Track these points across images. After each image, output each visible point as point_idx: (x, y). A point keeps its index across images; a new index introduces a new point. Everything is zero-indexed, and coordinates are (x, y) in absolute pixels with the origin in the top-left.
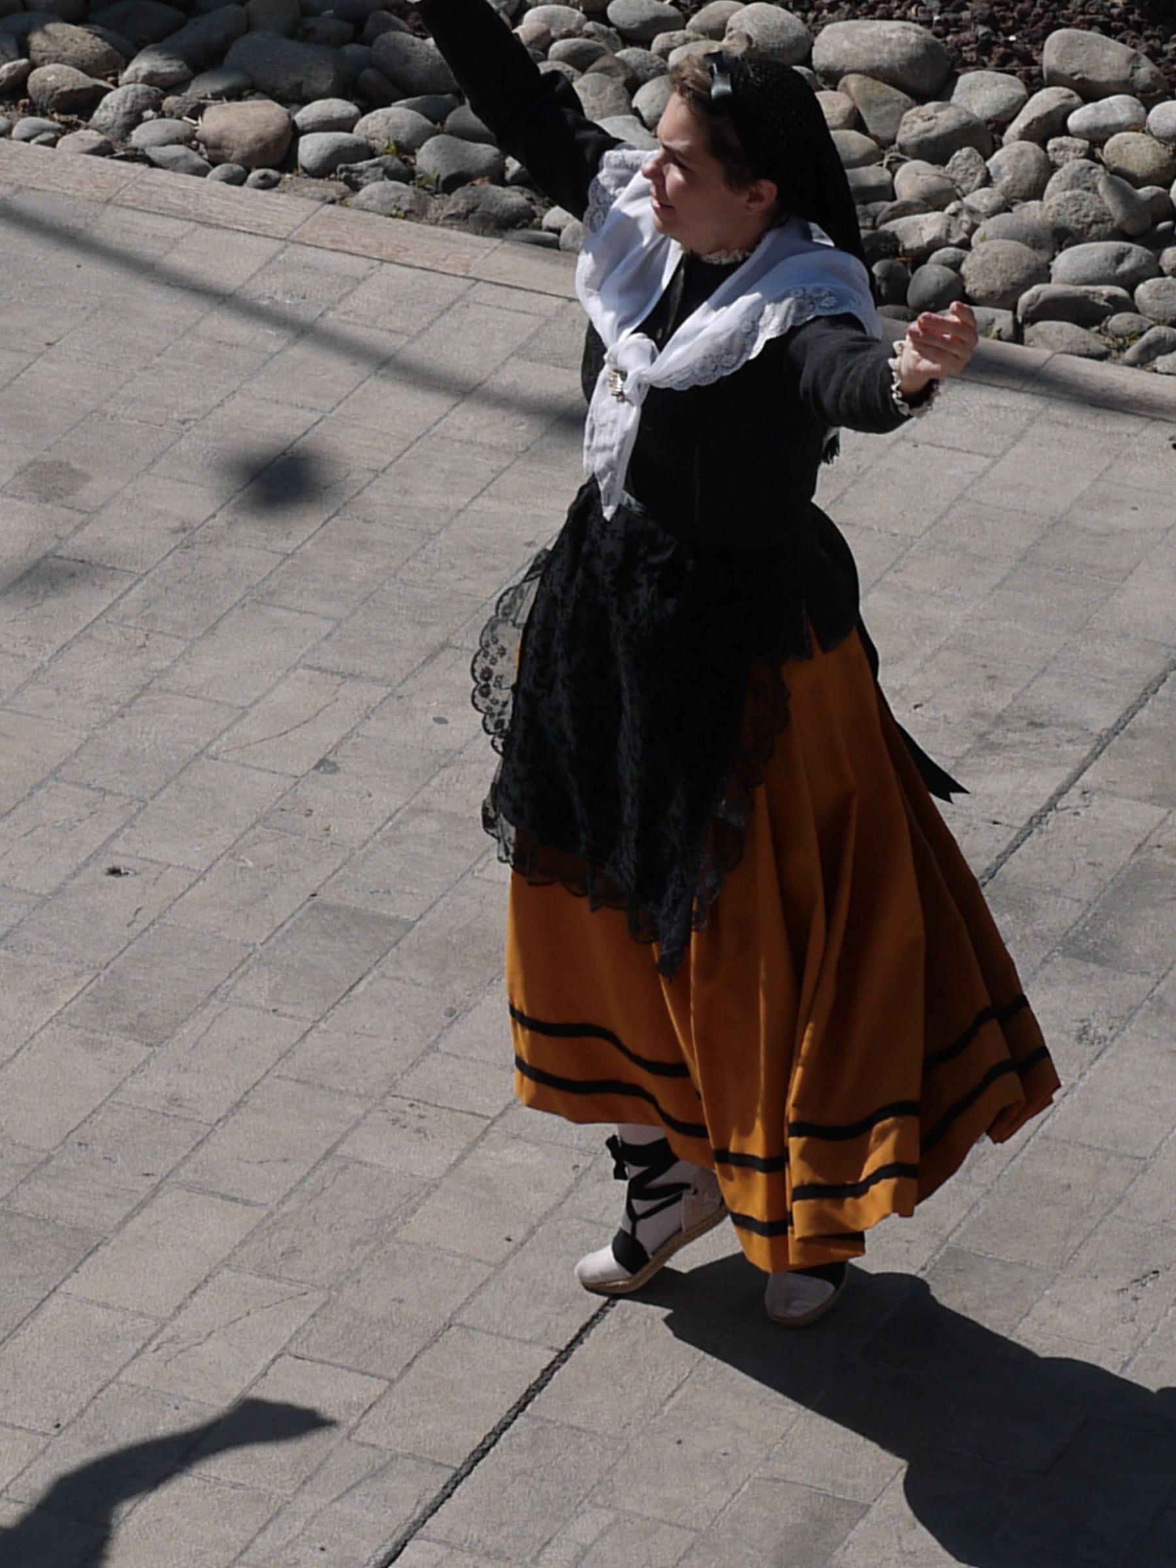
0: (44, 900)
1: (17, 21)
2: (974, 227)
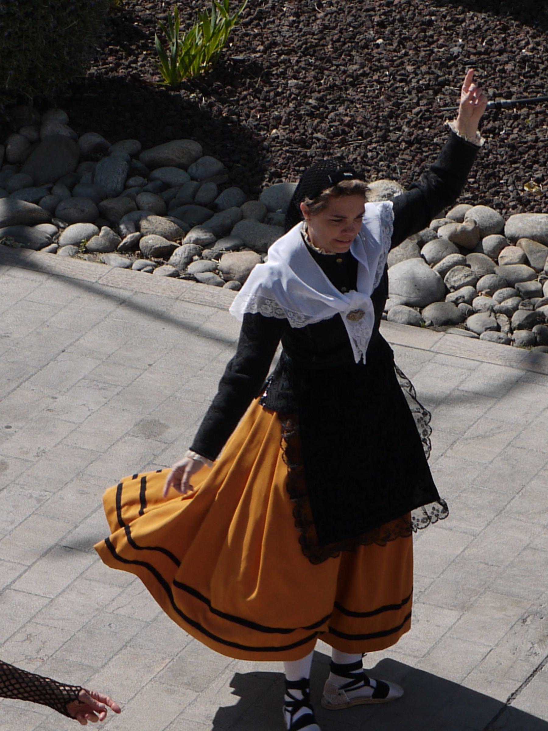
0: (148, 624)
1: (135, 215)
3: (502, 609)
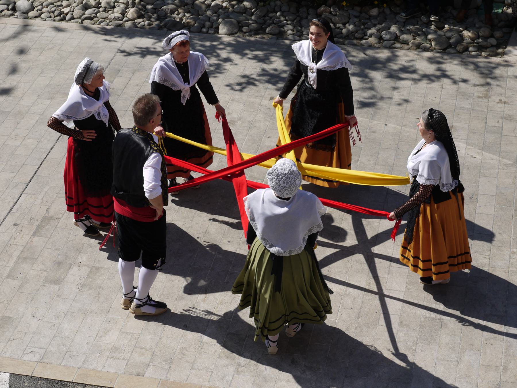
2: (74, 9)
3: (63, 97)
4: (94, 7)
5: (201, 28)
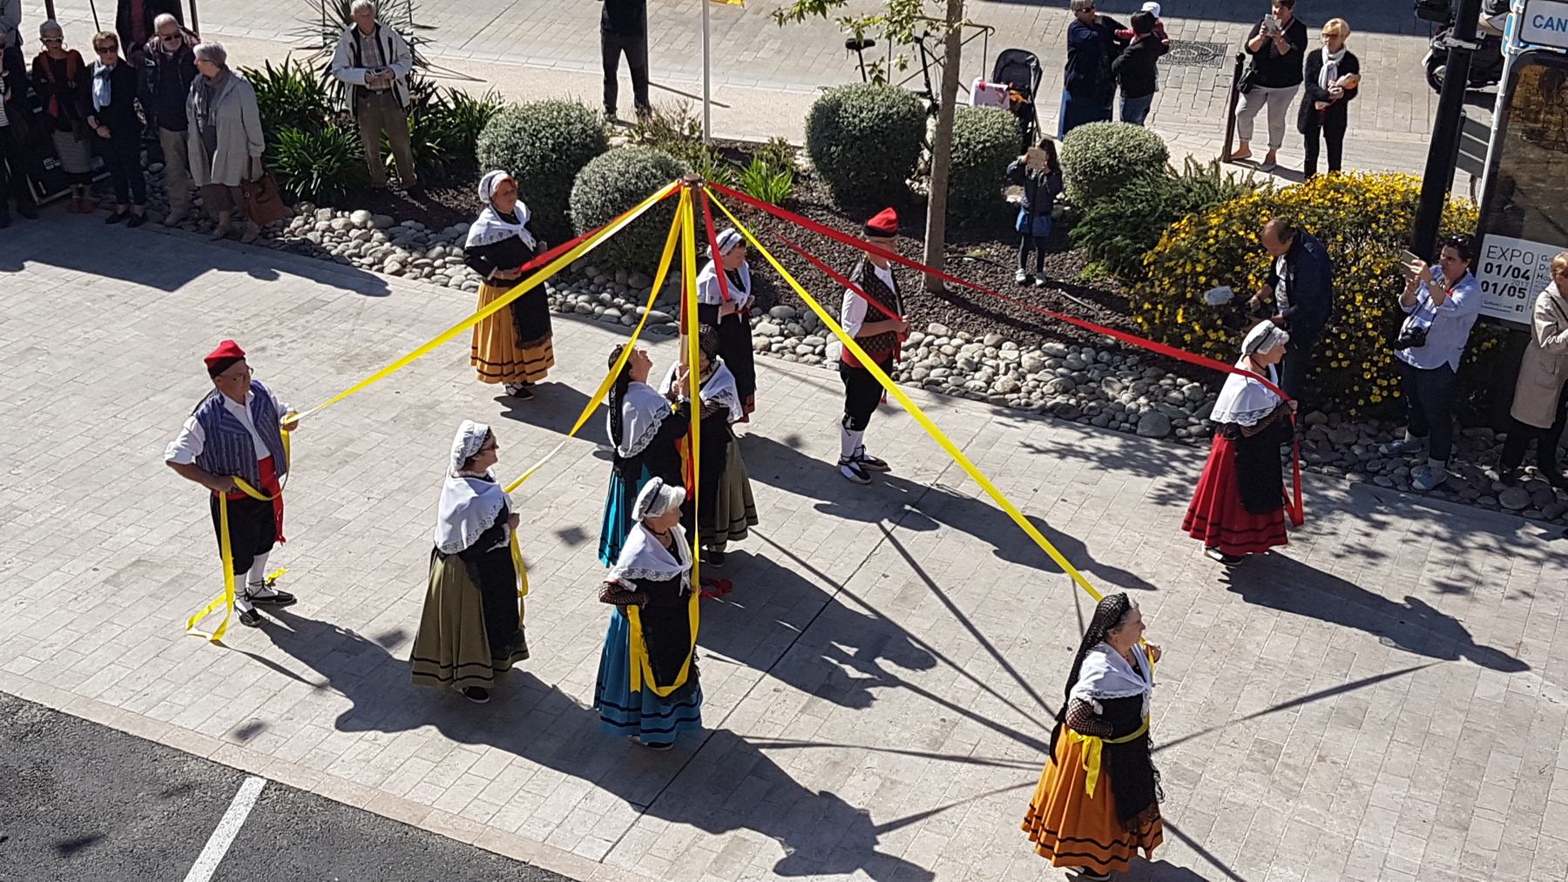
4: (944, 367)
5: (1109, 421)
